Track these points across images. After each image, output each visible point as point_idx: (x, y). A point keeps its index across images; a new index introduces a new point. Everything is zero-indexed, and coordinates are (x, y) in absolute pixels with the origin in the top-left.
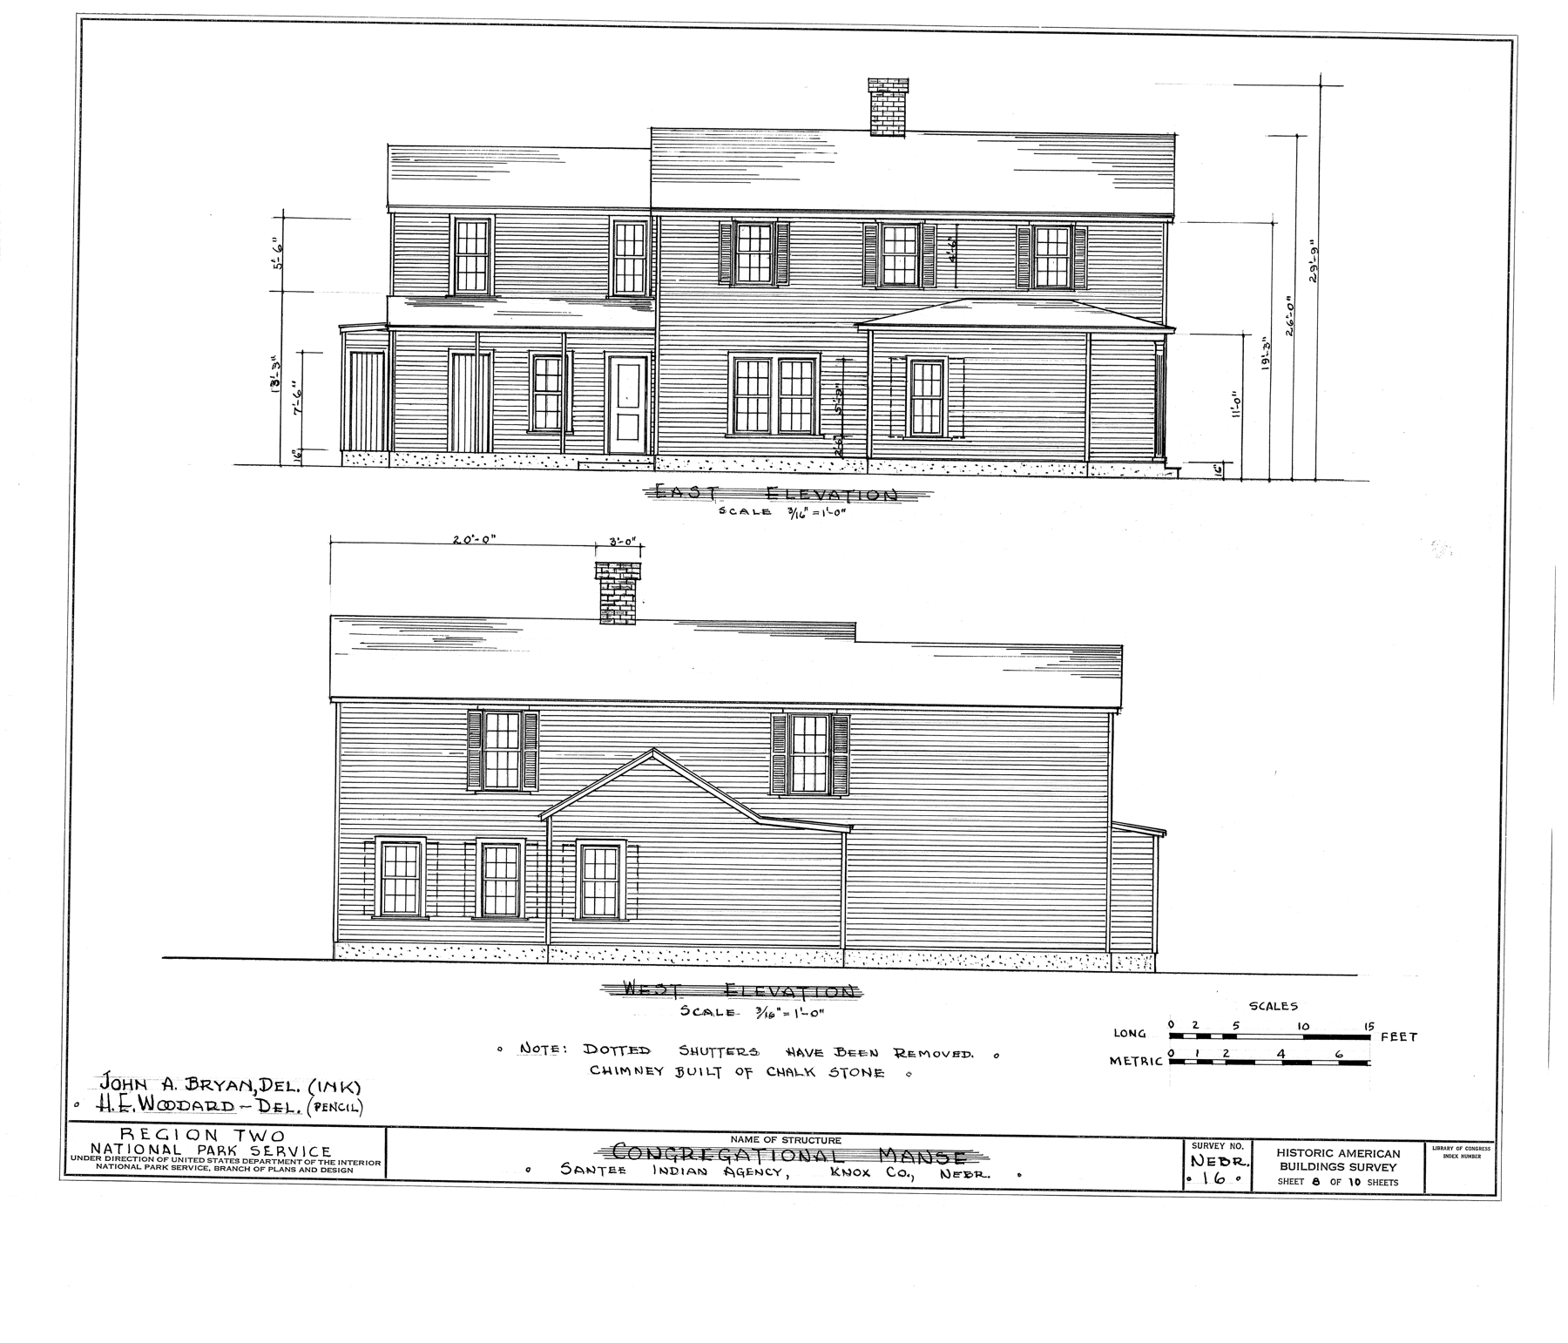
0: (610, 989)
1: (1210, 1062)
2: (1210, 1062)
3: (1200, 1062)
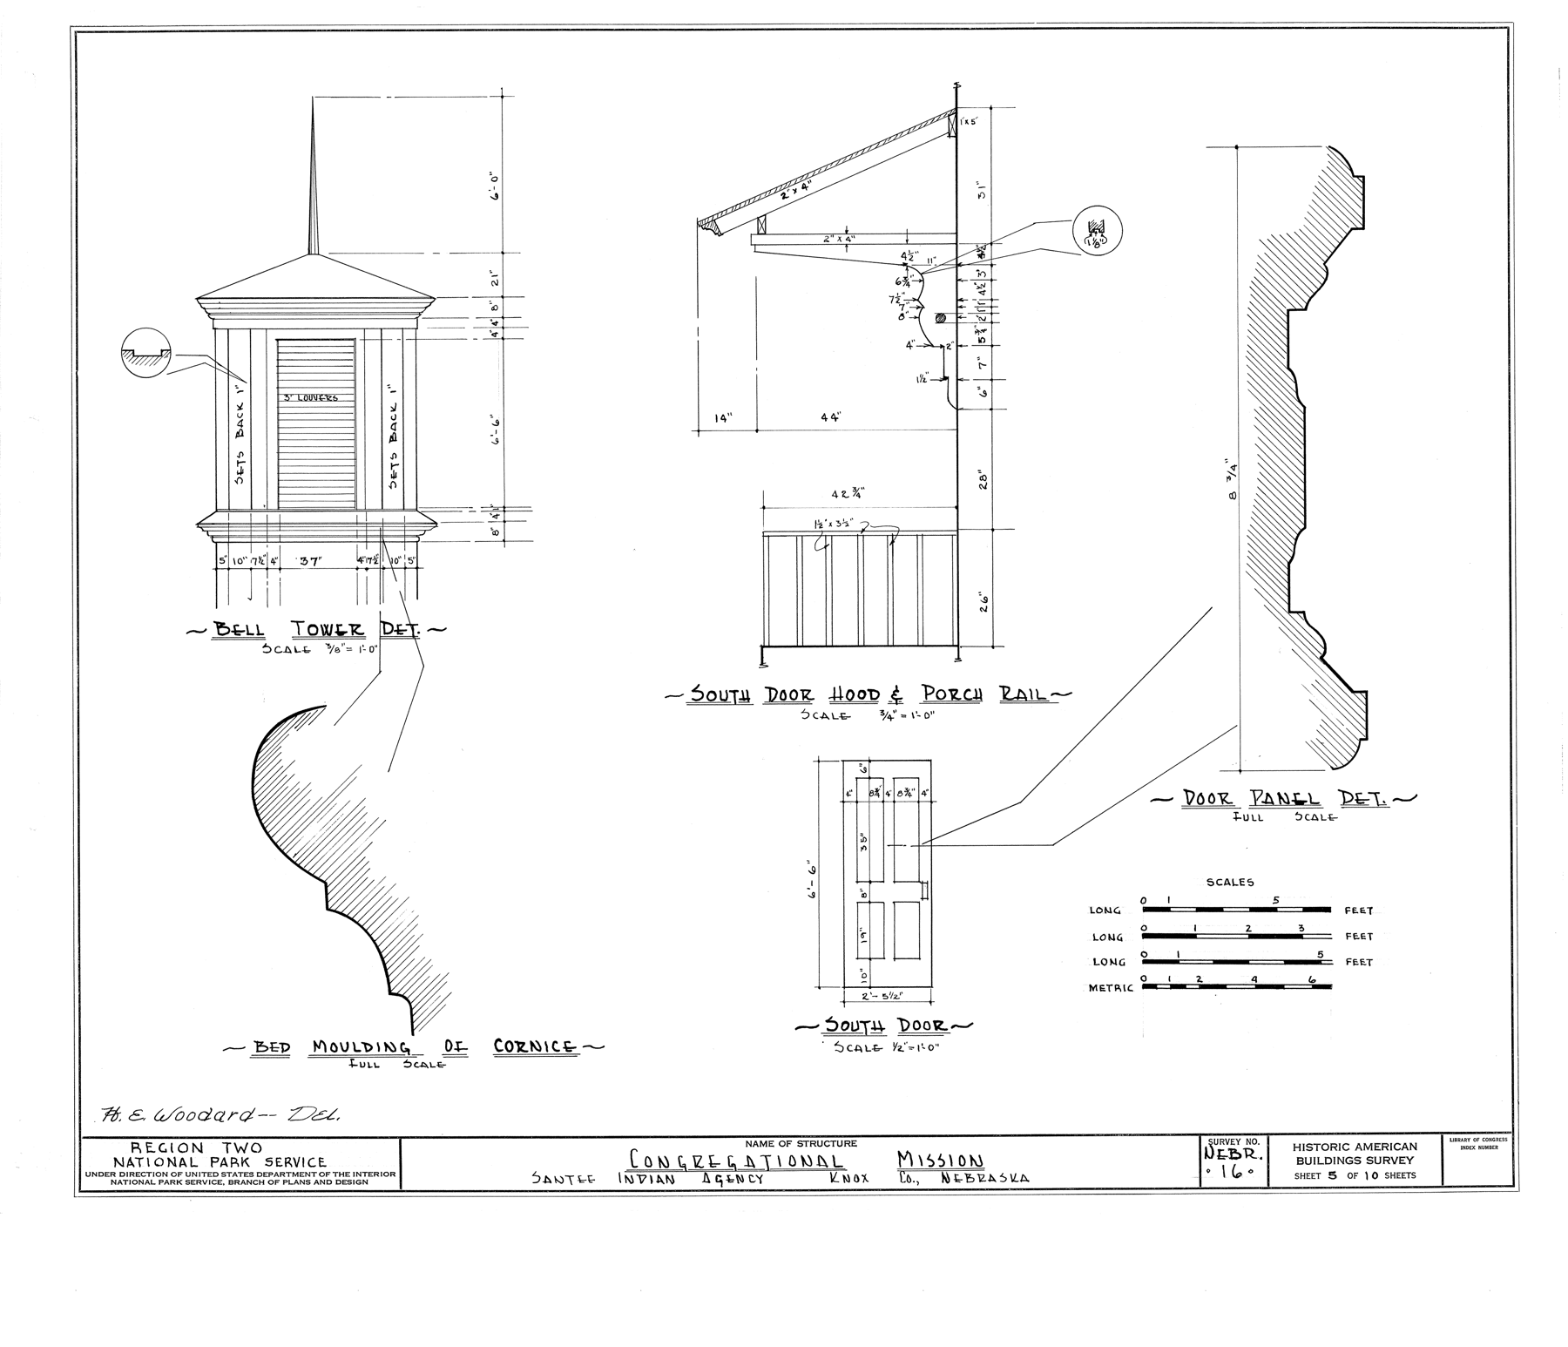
0: (688, 704)
1: (1183, 986)
2: (1183, 986)
3: (1173, 986)
